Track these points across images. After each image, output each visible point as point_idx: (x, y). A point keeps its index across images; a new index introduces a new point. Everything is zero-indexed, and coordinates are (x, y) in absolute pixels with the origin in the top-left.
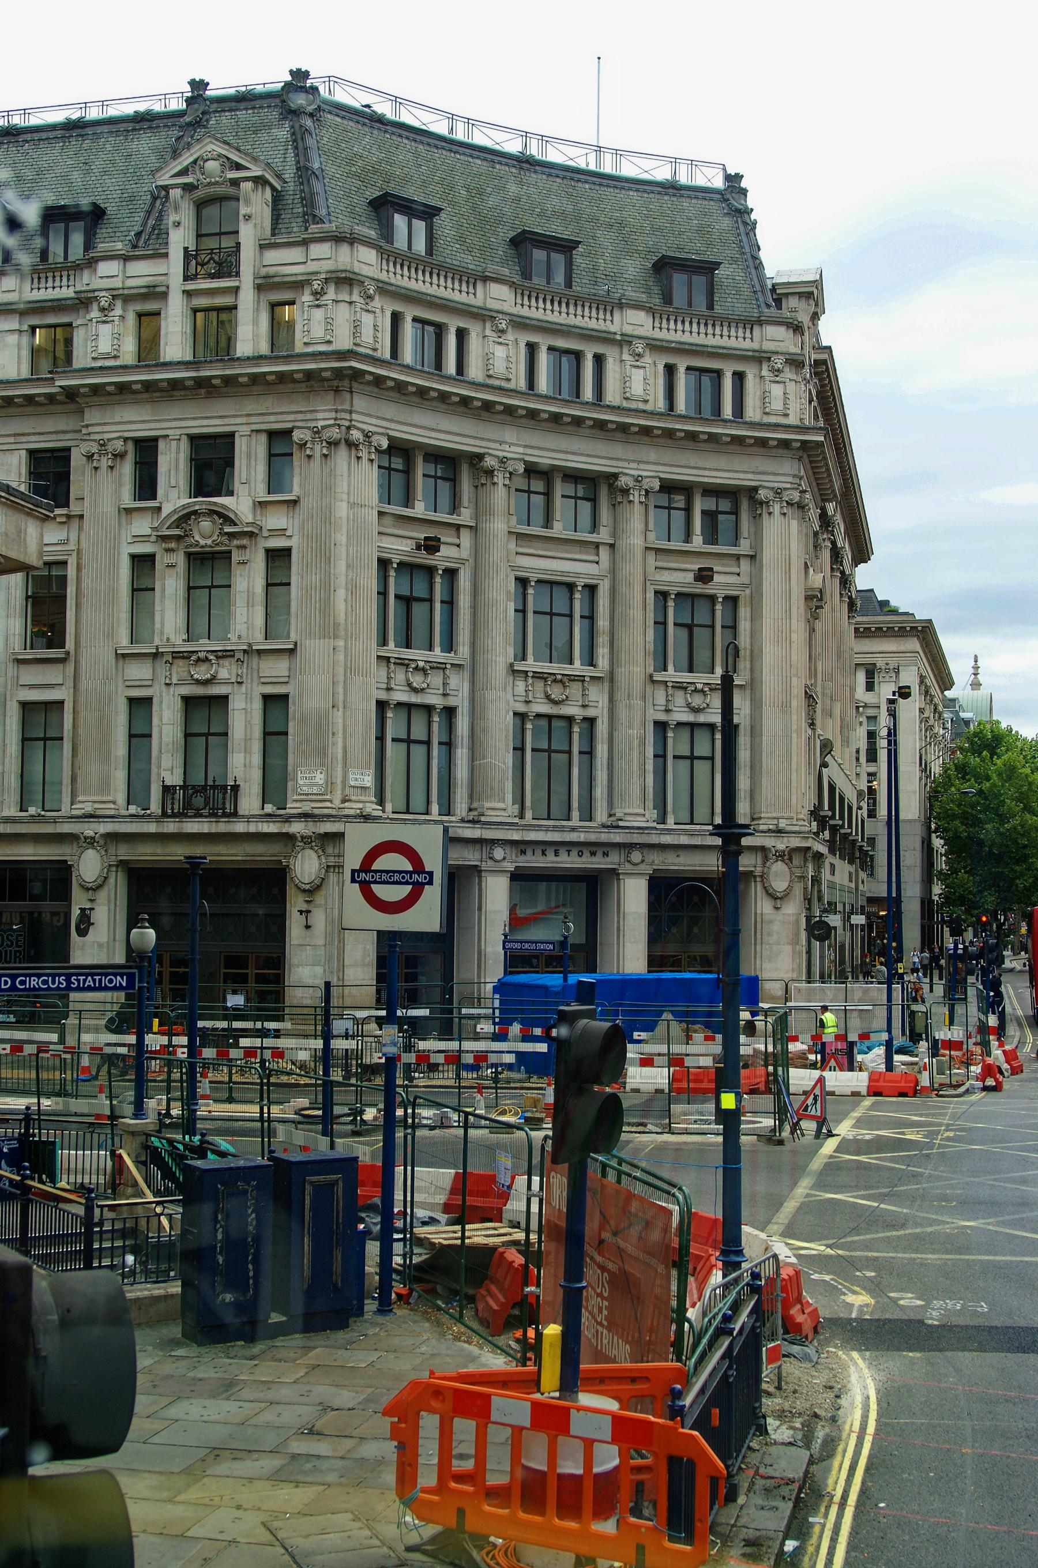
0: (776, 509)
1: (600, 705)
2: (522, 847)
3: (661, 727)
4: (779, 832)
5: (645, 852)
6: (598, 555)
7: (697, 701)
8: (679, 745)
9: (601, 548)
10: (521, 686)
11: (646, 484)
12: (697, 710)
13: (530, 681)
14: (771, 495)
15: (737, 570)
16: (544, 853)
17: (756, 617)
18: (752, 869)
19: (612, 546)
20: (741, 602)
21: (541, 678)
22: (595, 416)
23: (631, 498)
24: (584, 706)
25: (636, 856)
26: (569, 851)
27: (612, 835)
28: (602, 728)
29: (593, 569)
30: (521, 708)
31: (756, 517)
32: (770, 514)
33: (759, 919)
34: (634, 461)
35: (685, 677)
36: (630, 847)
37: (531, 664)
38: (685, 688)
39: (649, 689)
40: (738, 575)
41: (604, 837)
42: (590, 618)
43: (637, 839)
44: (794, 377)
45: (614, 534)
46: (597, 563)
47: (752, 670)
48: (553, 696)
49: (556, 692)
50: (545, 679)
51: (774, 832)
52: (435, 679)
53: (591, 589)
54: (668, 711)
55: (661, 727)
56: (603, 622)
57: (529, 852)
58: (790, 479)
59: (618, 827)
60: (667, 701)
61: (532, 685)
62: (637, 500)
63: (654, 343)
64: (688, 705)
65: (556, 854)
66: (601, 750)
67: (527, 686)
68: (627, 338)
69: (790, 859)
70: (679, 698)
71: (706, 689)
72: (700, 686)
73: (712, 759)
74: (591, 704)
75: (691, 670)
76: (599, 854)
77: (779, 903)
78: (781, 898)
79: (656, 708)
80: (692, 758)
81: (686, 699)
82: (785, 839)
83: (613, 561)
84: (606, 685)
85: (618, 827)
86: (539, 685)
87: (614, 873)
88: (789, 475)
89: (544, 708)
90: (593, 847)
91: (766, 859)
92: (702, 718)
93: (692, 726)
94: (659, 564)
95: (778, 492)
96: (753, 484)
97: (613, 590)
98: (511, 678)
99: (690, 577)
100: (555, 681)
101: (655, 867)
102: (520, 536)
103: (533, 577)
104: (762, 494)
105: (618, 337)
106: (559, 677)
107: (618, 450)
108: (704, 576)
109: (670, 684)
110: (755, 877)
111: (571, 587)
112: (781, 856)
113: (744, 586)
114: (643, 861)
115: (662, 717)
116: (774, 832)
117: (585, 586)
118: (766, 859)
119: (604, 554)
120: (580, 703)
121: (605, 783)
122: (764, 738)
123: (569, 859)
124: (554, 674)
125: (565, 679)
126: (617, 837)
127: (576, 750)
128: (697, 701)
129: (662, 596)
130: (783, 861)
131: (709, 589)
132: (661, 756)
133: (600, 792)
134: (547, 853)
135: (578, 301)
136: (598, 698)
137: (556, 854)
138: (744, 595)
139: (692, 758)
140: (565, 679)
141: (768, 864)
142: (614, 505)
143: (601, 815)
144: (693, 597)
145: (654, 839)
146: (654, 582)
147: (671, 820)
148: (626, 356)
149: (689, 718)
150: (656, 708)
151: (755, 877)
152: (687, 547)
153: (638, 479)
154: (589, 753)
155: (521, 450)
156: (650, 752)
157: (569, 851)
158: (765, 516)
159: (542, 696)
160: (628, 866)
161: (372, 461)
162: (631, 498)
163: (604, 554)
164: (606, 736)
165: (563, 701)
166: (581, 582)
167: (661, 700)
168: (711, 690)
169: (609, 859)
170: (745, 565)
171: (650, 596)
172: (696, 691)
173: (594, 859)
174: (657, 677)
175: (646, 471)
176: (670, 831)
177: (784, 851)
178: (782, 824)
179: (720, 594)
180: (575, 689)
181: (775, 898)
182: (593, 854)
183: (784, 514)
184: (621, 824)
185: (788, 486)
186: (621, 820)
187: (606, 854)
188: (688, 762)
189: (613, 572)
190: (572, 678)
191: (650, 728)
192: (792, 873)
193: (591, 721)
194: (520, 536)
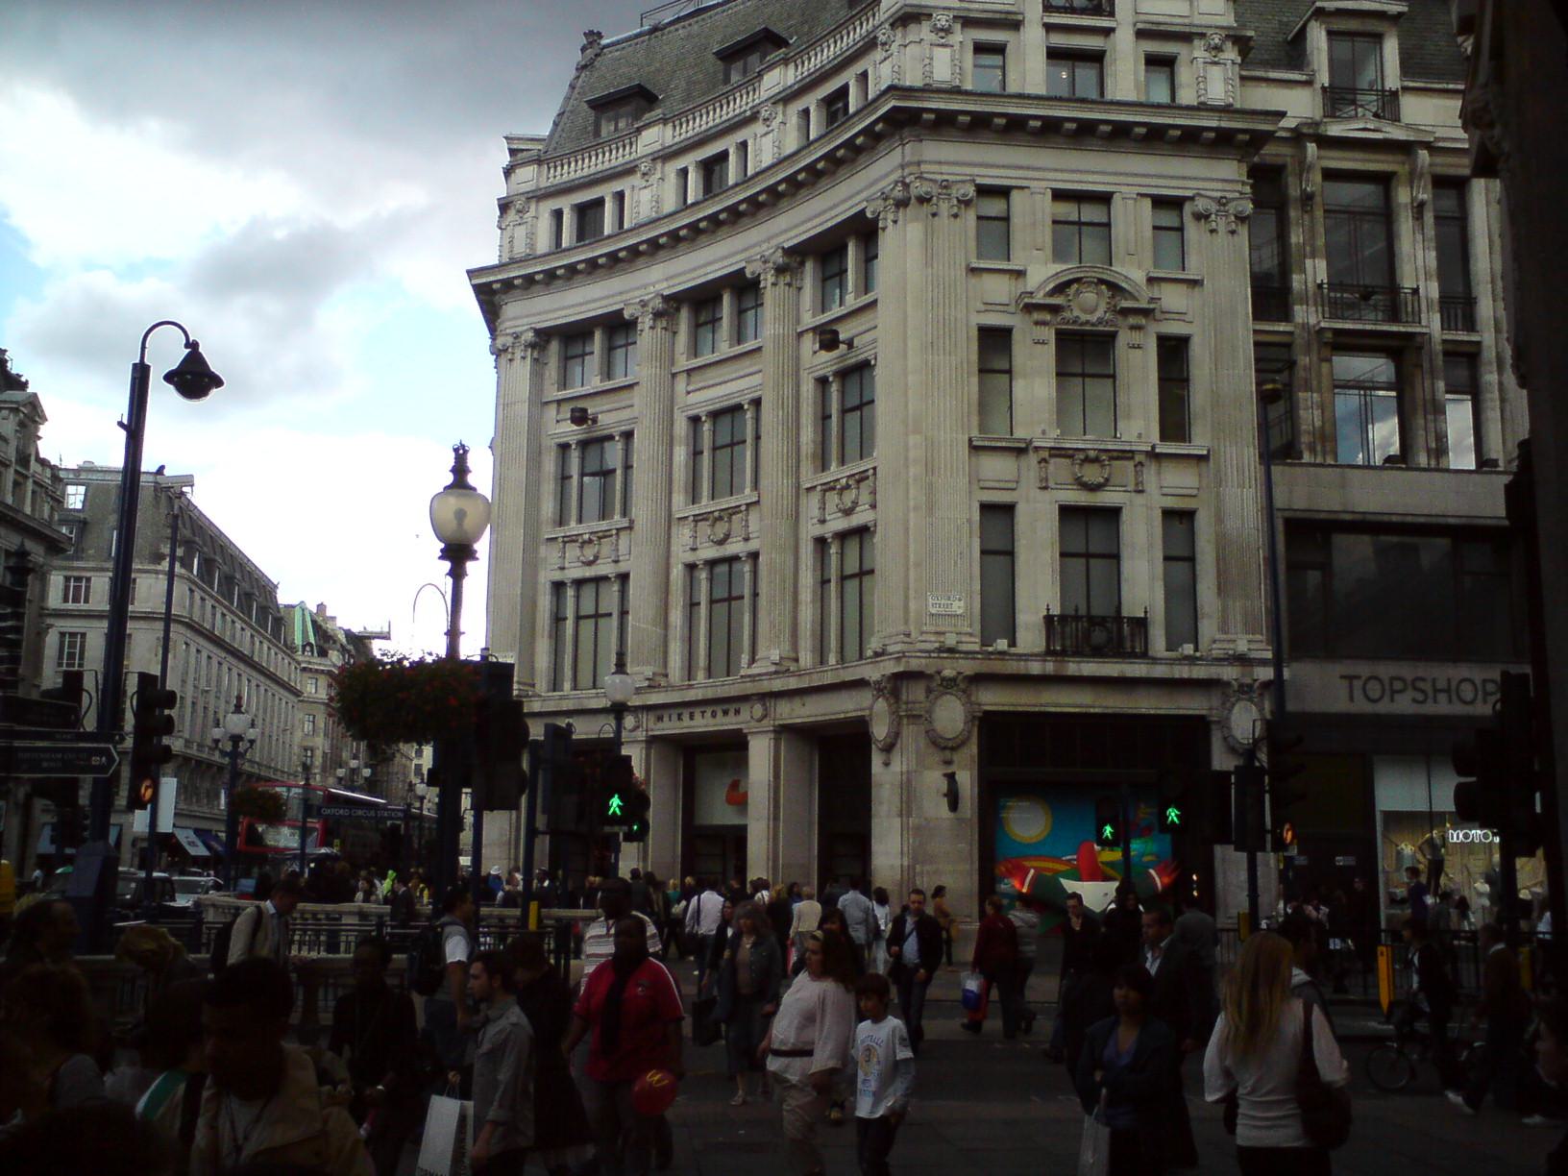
2: (659, 712)
5: (772, 703)
16: (680, 718)
37: (706, 505)
52: (606, 548)
57: (686, 717)
65: (692, 717)
69: (895, 694)
103: (701, 411)
105: (748, 113)
111: (738, 408)
137: (692, 717)
155: (665, 285)
157: (703, 713)
161: (524, 358)
182: (726, 713)
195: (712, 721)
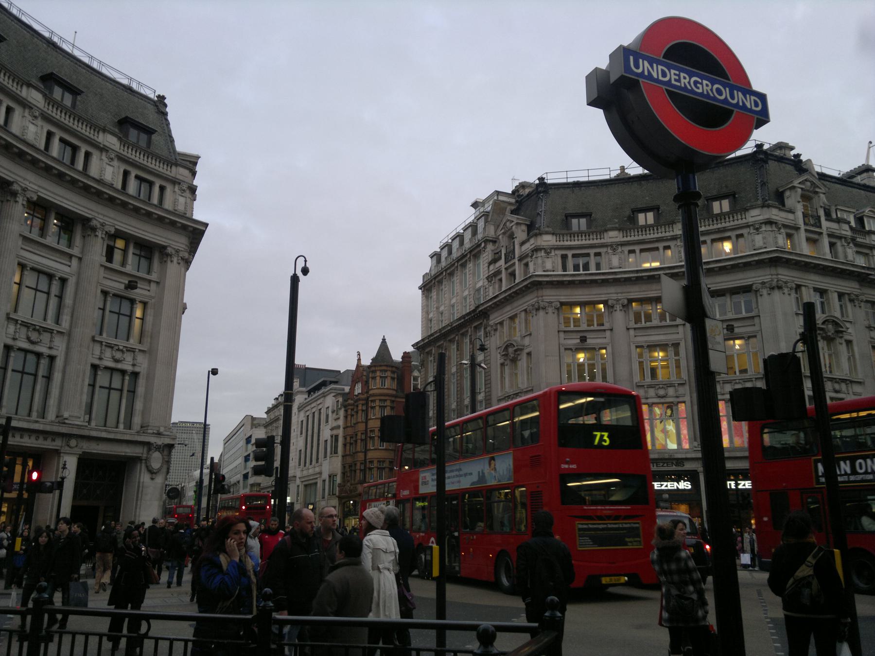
0: (175, 259)
1: (60, 349)
3: (95, 367)
4: (159, 434)
6: (71, 262)
7: (118, 355)
8: (103, 379)
9: (73, 258)
10: (12, 328)
11: (107, 228)
12: (117, 361)
13: (18, 326)
14: (173, 252)
15: (148, 288)
17: (158, 315)
18: (141, 455)
19: (80, 259)
20: (149, 306)
21: (26, 326)
22: (85, 181)
23: (97, 233)
24: (50, 348)
25: (73, 442)
26: (30, 436)
27: (60, 428)
28: (59, 363)
29: (67, 269)
30: (10, 342)
31: (163, 262)
32: (172, 261)
33: (141, 485)
34: (102, 214)
35: (113, 341)
36: (68, 436)
38: (112, 348)
39: (91, 345)
40: (149, 291)
41: (55, 429)
42: (60, 297)
43: (75, 431)
44: (190, 197)
45: (82, 252)
46: (70, 266)
47: (151, 343)
48: (32, 339)
49: (34, 336)
50: (28, 327)
51: (156, 434)
53: (63, 281)
54: (100, 359)
55: (95, 367)
56: (68, 300)
58: (184, 246)
59: (64, 423)
60: (101, 353)
61: (19, 329)
62: (100, 236)
63: (121, 155)
64: (113, 358)
65: (21, 437)
66: (57, 376)
67: (16, 329)
68: (106, 148)
69: (163, 450)
70: (108, 353)
71: (125, 350)
72: (121, 348)
73: (121, 390)
74: (55, 347)
75: (116, 338)
76: (49, 440)
77: (154, 476)
78: (155, 473)
79: (94, 356)
80: (110, 389)
81: (112, 354)
82: (162, 439)
83: (80, 268)
84: (66, 338)
85: (64, 423)
86: (24, 330)
87: (57, 452)
88: (183, 244)
89: (25, 345)
90: (45, 434)
91: (149, 450)
92: (119, 366)
93: (112, 370)
94: (106, 276)
95: (177, 251)
96: (164, 244)
97: (77, 284)
98: (6, 322)
99: (122, 287)
100: (34, 330)
101: (83, 450)
102: (25, 239)
104: (169, 250)
105: (102, 146)
106: (38, 327)
107: (92, 205)
108: (131, 286)
109: (104, 343)
110: (141, 460)
111: (50, 277)
112: (159, 448)
113: (152, 297)
114: (76, 446)
115: (97, 362)
116: (156, 434)
117: (60, 278)
118: (149, 450)
119: (75, 262)
120: (48, 346)
121: (57, 396)
122: (156, 381)
123: (29, 441)
124: (35, 325)
125: (41, 330)
126: (63, 430)
127: (41, 373)
128: (118, 355)
129: (105, 293)
130: (159, 451)
131: (133, 294)
132: (92, 386)
133: (52, 401)
134: (16, 436)
135: (80, 119)
136: (60, 345)
138: (151, 302)
139: (110, 389)
140: (41, 330)
141: (151, 453)
142: (84, 237)
143: (51, 415)
144: (122, 297)
145: (85, 433)
146: (101, 284)
147: (93, 424)
148: (104, 157)
149: (112, 364)
150: (94, 356)
151: (141, 460)
152: (123, 269)
153: (103, 225)
154: (48, 378)
156: (87, 382)
157: (30, 436)
158: (169, 262)
159: (25, 337)
160: (67, 448)
162: (97, 233)
163: (75, 262)
164: (61, 368)
165: (38, 342)
166: (59, 275)
167: (97, 351)
168: (127, 351)
169: (54, 443)
170: (153, 286)
171: (99, 291)
172: (118, 350)
173: (45, 443)
174: (97, 339)
175: (108, 221)
176: (91, 429)
177: (160, 446)
178: (162, 429)
179: (138, 299)
180: (46, 337)
181: (152, 472)
182: (45, 439)
183: (179, 263)
184: (66, 421)
185: (183, 249)
186: (66, 419)
187: (53, 440)
188: (107, 391)
189: (79, 274)
190: (46, 330)
191: (89, 367)
192: (163, 459)
193: (52, 358)
194: (25, 239)
195: (35, 442)
